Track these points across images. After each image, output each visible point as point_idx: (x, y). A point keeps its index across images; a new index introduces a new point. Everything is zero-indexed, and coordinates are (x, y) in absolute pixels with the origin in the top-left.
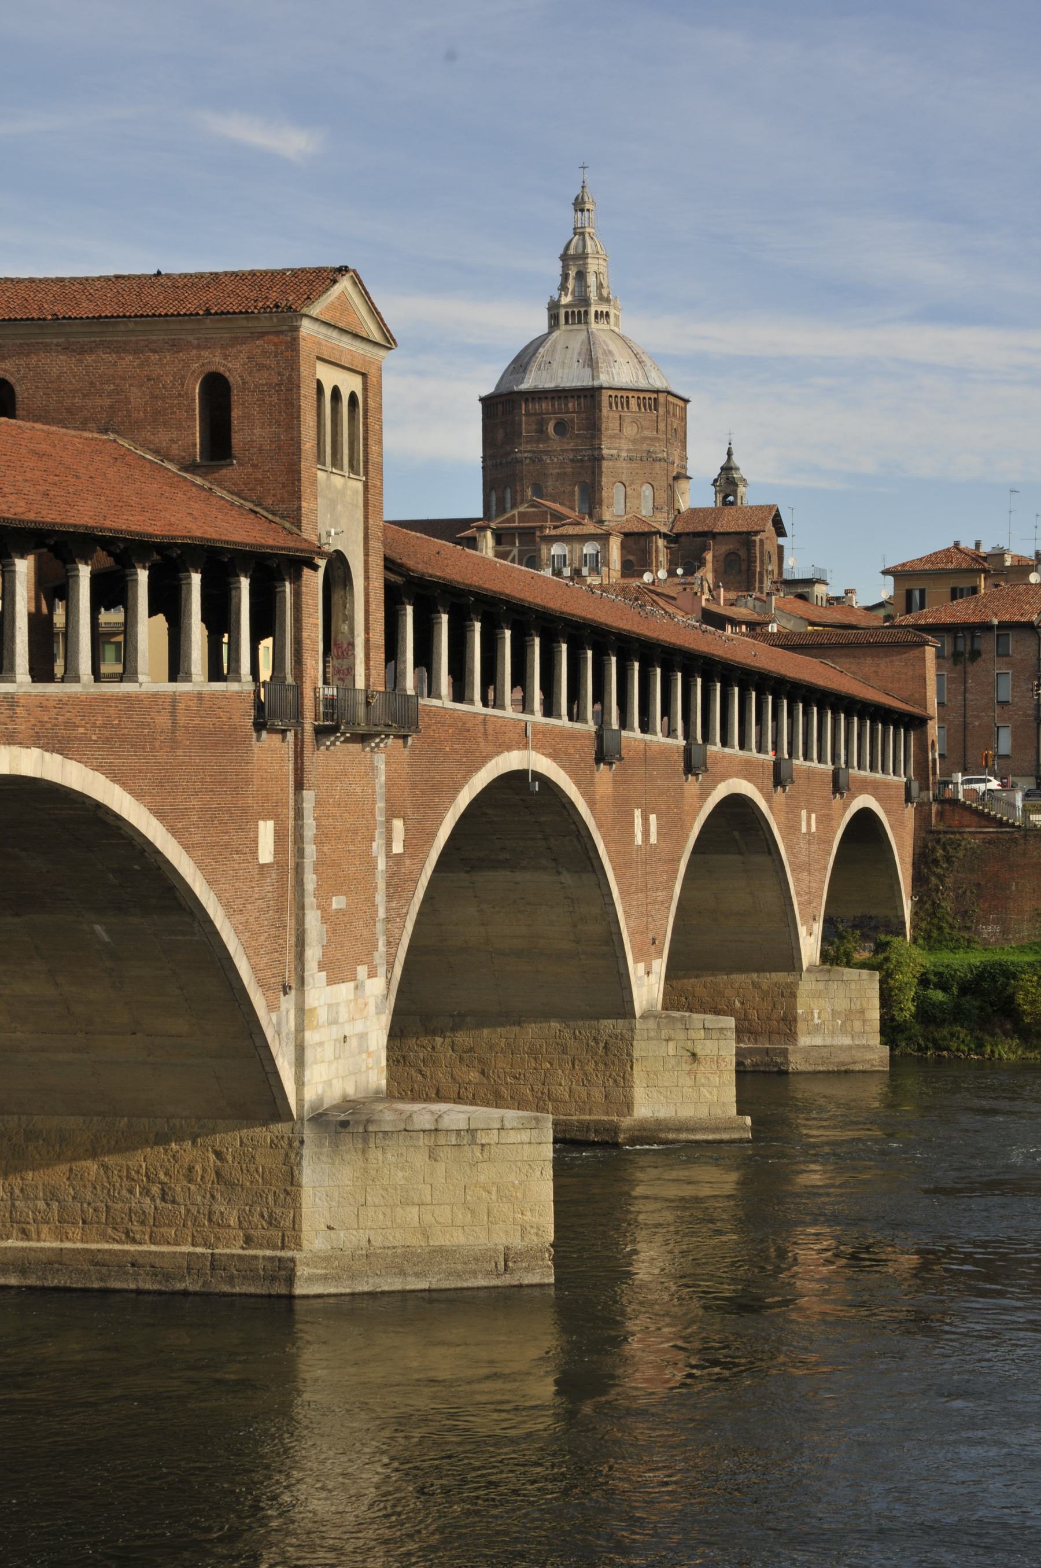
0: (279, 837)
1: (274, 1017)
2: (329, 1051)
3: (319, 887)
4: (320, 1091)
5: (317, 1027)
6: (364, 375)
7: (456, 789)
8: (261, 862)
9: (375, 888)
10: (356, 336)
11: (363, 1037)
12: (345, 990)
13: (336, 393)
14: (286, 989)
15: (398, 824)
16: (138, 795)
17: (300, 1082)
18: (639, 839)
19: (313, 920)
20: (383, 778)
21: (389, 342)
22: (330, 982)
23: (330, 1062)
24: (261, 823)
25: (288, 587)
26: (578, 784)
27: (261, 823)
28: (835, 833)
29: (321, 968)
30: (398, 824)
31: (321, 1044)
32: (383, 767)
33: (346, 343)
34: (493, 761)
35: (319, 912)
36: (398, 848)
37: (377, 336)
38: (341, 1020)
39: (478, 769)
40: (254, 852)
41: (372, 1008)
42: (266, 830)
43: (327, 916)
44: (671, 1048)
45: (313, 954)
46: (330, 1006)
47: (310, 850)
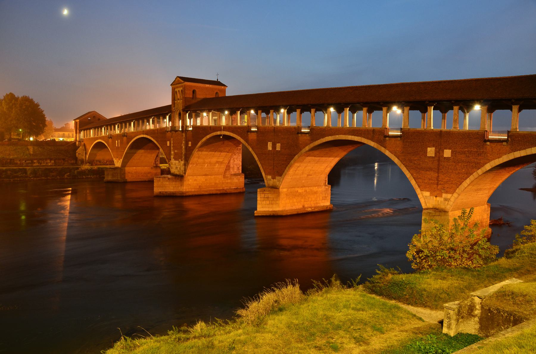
0: (170, 143)
2: (175, 168)
3: (173, 149)
7: (203, 138)
9: (182, 150)
11: (180, 168)
12: (177, 162)
13: (179, 91)
15: (190, 143)
18: (270, 148)
19: (172, 152)
22: (175, 160)
26: (241, 137)
29: (173, 158)
30: (190, 143)
33: (178, 85)
34: (212, 134)
36: (190, 145)
39: (208, 135)
41: (182, 164)
42: (168, 142)
43: (174, 153)
45: (172, 157)
46: (175, 163)
47: (172, 145)
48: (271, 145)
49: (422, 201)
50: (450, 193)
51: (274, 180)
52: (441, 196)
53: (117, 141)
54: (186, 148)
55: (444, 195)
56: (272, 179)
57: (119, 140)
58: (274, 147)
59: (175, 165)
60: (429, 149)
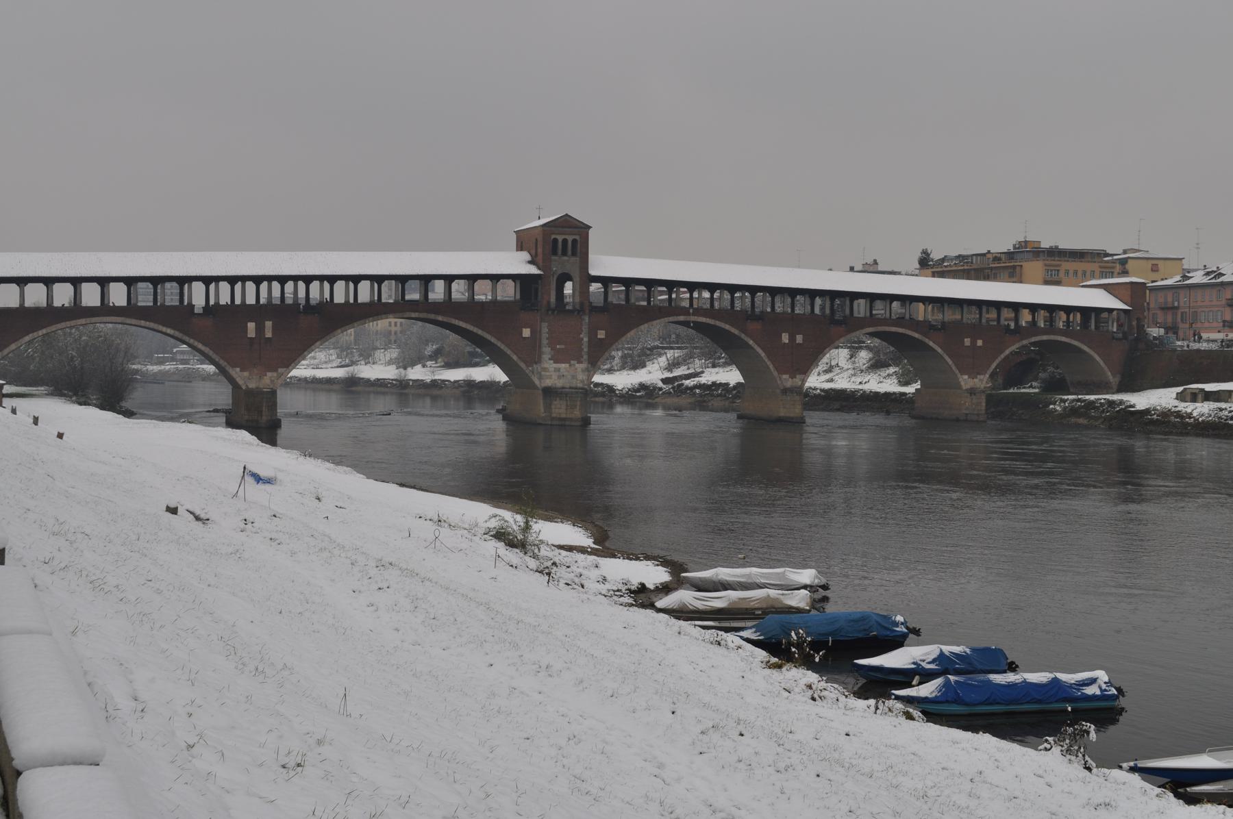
1: (530, 368)
4: (550, 385)
5: (548, 371)
6: (579, 235)
8: (524, 336)
10: (570, 227)
11: (574, 377)
12: (563, 366)
13: (565, 241)
14: (536, 363)
16: (466, 322)
17: (541, 382)
20: (587, 321)
21: (590, 227)
23: (555, 380)
24: (524, 330)
25: (540, 281)
27: (524, 330)
28: (1008, 348)
31: (551, 375)
32: (587, 318)
35: (550, 349)
37: (583, 226)
38: (561, 371)
40: (521, 333)
41: (579, 370)
44: (789, 398)
45: (546, 357)
46: (555, 368)
48: (787, 337)
49: (963, 383)
50: (982, 374)
51: (794, 379)
52: (976, 378)
53: (251, 326)
54: (589, 341)
55: (978, 376)
56: (790, 379)
57: (269, 324)
58: (792, 338)
59: (558, 370)
60: (966, 340)
